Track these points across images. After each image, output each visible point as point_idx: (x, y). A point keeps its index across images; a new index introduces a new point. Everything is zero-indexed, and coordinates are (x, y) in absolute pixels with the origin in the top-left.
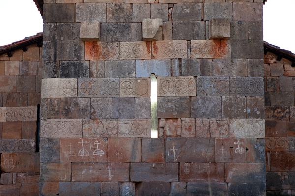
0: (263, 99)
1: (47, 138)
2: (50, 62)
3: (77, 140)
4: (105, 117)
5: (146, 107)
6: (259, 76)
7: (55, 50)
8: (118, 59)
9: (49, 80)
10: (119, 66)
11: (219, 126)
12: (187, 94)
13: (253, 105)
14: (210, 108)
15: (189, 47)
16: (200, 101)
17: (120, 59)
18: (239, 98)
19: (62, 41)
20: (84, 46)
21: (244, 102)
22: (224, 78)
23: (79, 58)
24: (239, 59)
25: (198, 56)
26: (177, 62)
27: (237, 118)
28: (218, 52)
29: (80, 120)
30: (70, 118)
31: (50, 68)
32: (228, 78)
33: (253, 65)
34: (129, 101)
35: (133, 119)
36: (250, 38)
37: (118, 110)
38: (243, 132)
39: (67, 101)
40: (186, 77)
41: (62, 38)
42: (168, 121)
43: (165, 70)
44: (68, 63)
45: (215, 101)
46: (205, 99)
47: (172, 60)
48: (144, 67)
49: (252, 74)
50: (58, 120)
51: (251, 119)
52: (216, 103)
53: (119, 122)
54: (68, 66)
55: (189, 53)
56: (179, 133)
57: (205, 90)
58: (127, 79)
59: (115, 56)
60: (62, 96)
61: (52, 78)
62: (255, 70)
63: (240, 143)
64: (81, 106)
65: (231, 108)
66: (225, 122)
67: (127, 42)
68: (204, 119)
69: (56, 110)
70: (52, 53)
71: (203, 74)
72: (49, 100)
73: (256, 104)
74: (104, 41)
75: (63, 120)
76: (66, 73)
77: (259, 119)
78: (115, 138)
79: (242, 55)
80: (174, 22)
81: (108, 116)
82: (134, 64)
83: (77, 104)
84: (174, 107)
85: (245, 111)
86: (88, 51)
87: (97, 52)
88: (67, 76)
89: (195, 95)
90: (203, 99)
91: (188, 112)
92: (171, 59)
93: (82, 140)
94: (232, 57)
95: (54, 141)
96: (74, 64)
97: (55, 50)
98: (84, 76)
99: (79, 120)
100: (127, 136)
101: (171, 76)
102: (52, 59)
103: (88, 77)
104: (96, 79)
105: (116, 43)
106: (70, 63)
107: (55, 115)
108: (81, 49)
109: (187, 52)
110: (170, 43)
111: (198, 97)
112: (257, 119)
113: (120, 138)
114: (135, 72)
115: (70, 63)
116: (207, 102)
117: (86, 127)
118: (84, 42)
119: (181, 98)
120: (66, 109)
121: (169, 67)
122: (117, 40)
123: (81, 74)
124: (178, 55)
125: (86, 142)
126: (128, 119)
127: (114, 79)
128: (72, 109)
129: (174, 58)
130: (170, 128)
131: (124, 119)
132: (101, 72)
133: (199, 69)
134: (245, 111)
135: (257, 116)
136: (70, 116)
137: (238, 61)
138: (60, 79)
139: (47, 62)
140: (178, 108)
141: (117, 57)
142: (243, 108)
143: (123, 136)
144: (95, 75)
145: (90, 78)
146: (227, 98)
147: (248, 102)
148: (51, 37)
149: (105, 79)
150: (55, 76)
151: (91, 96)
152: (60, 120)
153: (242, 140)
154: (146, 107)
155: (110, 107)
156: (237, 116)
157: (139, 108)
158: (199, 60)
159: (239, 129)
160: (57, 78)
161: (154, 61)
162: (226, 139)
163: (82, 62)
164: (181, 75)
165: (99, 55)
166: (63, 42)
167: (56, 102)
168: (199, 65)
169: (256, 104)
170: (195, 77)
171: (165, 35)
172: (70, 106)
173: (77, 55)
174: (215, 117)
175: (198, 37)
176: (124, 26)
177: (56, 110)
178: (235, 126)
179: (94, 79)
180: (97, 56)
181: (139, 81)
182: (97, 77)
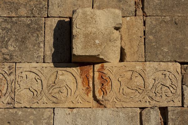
8: (11, 105)
17: (16, 106)
47: (144, 112)
67: (34, 64)
80: (148, 20)
82: (49, 118)
105: (7, 65)
109: (179, 92)
110: (138, 67)
124: (158, 99)
129: (147, 105)
171: (127, 51)
176: (28, 26)
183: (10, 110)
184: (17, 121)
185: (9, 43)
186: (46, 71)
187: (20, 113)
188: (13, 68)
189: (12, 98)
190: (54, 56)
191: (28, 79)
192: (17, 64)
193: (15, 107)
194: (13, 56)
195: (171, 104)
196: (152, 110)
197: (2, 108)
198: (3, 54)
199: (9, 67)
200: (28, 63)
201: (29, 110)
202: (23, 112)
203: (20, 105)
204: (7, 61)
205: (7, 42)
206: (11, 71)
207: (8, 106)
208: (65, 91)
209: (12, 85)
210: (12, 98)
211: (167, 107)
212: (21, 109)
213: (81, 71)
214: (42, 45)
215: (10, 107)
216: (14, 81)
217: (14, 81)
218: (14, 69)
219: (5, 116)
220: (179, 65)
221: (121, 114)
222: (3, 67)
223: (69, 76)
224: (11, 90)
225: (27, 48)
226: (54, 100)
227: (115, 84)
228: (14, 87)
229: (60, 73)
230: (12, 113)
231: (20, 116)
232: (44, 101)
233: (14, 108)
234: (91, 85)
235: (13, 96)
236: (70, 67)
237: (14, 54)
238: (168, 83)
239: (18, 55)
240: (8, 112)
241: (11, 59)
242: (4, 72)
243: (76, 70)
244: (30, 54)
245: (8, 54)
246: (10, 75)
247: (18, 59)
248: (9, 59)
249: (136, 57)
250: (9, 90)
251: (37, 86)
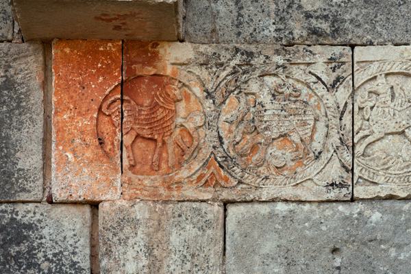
8: (343, 192)
10: (347, 251)
17: (360, 192)
20: (45, 84)
59: (312, 169)
74: (213, 36)
86: (76, 122)
87: (154, 130)
105: (321, 55)
108: (19, 105)
118: (46, 45)
163: (25, 213)
165: (171, 151)
180: (155, 168)
183: (341, 207)
184: (365, 244)
187: (376, 216)
188: (343, 63)
189: (344, 166)
191: (398, 101)
192: (356, 49)
193: (356, 195)
194: (344, 21)
197: (310, 202)
198: (308, 16)
199: (331, 60)
200: (396, 45)
202: (383, 213)
203: (372, 191)
204: (321, 40)
206: (338, 72)
207: (333, 195)
209: (343, 122)
210: (344, 166)
212: (377, 204)
215: (341, 197)
216: (350, 107)
217: (350, 107)
218: (347, 66)
219: (324, 228)
222: (307, 60)
224: (340, 139)
228: (349, 127)
230: (347, 218)
231: (373, 228)
233: (353, 200)
235: (349, 159)
237: (347, 17)
239: (359, 18)
240: (333, 215)
241: (336, 32)
242: (314, 79)
244: (403, 16)
245: (326, 17)
246: (333, 86)
247: (360, 32)
248: (328, 31)
250: (335, 139)
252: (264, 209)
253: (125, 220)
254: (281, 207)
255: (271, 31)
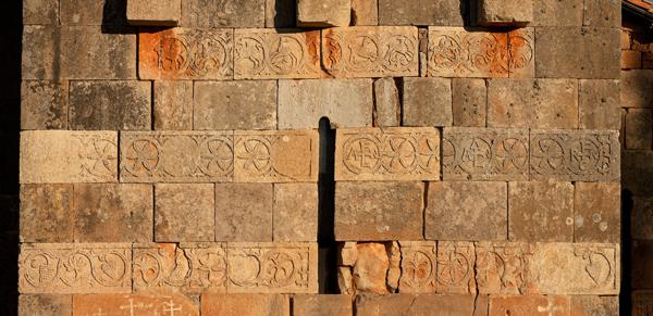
0: (616, 189)
1: (36, 296)
2: (42, 85)
3: (118, 301)
4: (191, 239)
5: (304, 211)
6: (608, 126)
7: (57, 51)
8: (230, 77)
9: (40, 134)
11: (500, 261)
12: (416, 177)
13: (590, 205)
14: (476, 216)
15: (423, 47)
16: (449, 195)
18: (554, 185)
19: (75, 25)
21: (567, 199)
22: (517, 131)
23: (121, 73)
24: (556, 81)
25: (447, 71)
26: (388, 91)
27: (547, 241)
28: (499, 59)
29: (125, 245)
30: (97, 240)
31: (42, 102)
32: (525, 131)
33: (592, 99)
34: (255, 193)
35: (270, 244)
36: (587, 23)
37: (229, 219)
38: (563, 279)
39: (88, 195)
40: (413, 129)
41: (76, 18)
42: (365, 249)
43: (358, 110)
44: (92, 87)
45: (492, 195)
46: (464, 188)
47: (377, 83)
48: (301, 101)
49: (590, 121)
50: (64, 245)
51: (586, 244)
52: (493, 200)
53: (231, 251)
54: (93, 95)
55: (424, 61)
56: (393, 282)
57: (463, 165)
58: (254, 133)
60: (76, 181)
61: (48, 128)
62: (598, 109)
63: (555, 309)
64: (128, 207)
65: (531, 213)
66: (517, 251)
67: (255, 30)
68: (460, 243)
69: (60, 217)
70: (49, 60)
71: (458, 120)
72: (40, 190)
73: (600, 202)
75: (77, 244)
76: (87, 114)
77: (606, 243)
78: (222, 295)
79: (564, 69)
81: (200, 234)
83: (116, 203)
84: (380, 211)
85: (570, 221)
88: (91, 124)
89: (438, 179)
90: (458, 190)
91: (418, 224)
92: (375, 79)
93: (131, 300)
94: (538, 74)
95: (55, 303)
96: (109, 92)
97: (57, 51)
98: (134, 121)
99: (120, 245)
100: (251, 289)
101: (374, 126)
102: (49, 76)
103: (149, 127)
104: (169, 132)
105: (224, 31)
106: (98, 88)
107: (59, 232)
109: (416, 59)
110: (371, 32)
111: (445, 184)
112: (603, 245)
113: (233, 296)
114: (274, 114)
115: (98, 88)
116: (470, 198)
117: (146, 264)
119: (398, 186)
120: (88, 215)
121: (370, 99)
122: (226, 23)
123: (127, 116)
124: (392, 67)
125: (141, 305)
126: (256, 244)
127: (219, 133)
128: (104, 214)
129: (381, 75)
130: (367, 268)
131: (245, 244)
132: (184, 112)
133: (448, 109)
134: (570, 221)
135: (601, 237)
136: (98, 232)
137: (553, 86)
138: (71, 132)
139: (33, 84)
140: (389, 211)
141: (227, 70)
142: (566, 213)
143: (242, 290)
144: (166, 122)
145: (153, 129)
146: (523, 185)
147: (578, 197)
148: (46, 13)
149: (195, 133)
150: (57, 122)
151: (156, 179)
152: (70, 245)
153: (558, 300)
154: (304, 211)
155: (207, 211)
156: (548, 235)
157: (284, 214)
158: (448, 83)
159: (552, 271)
160: (63, 127)
161: (328, 83)
162: (518, 299)
164: (401, 125)
166: (77, 28)
167: (59, 197)
168: (448, 97)
169: (600, 202)
170: (440, 129)
171: (358, 13)
172: (98, 206)
173: (118, 68)
174: (490, 238)
175: (446, 18)
177: (60, 217)
178: (543, 262)
179: (163, 133)
181: (286, 139)
182: (172, 127)
185: (226, 5)
186: (268, 37)
190: (276, 19)
195: (407, 73)
196: (386, 82)
201: (250, 82)
205: (224, 4)
208: (290, 60)
211: (402, 77)
213: (307, 36)
214: (263, 8)
220: (416, 29)
221: (351, 85)
223: (294, 43)
225: (245, 11)
226: (278, 71)
227: (345, 51)
229: (283, 39)
232: (267, 72)
234: (318, 53)
236: (296, 32)
238: (404, 50)
243: (301, 36)
249: (368, 21)
251: (258, 55)
252: (205, 83)
253: (162, 86)
254: (211, 83)
255: (207, 23)
